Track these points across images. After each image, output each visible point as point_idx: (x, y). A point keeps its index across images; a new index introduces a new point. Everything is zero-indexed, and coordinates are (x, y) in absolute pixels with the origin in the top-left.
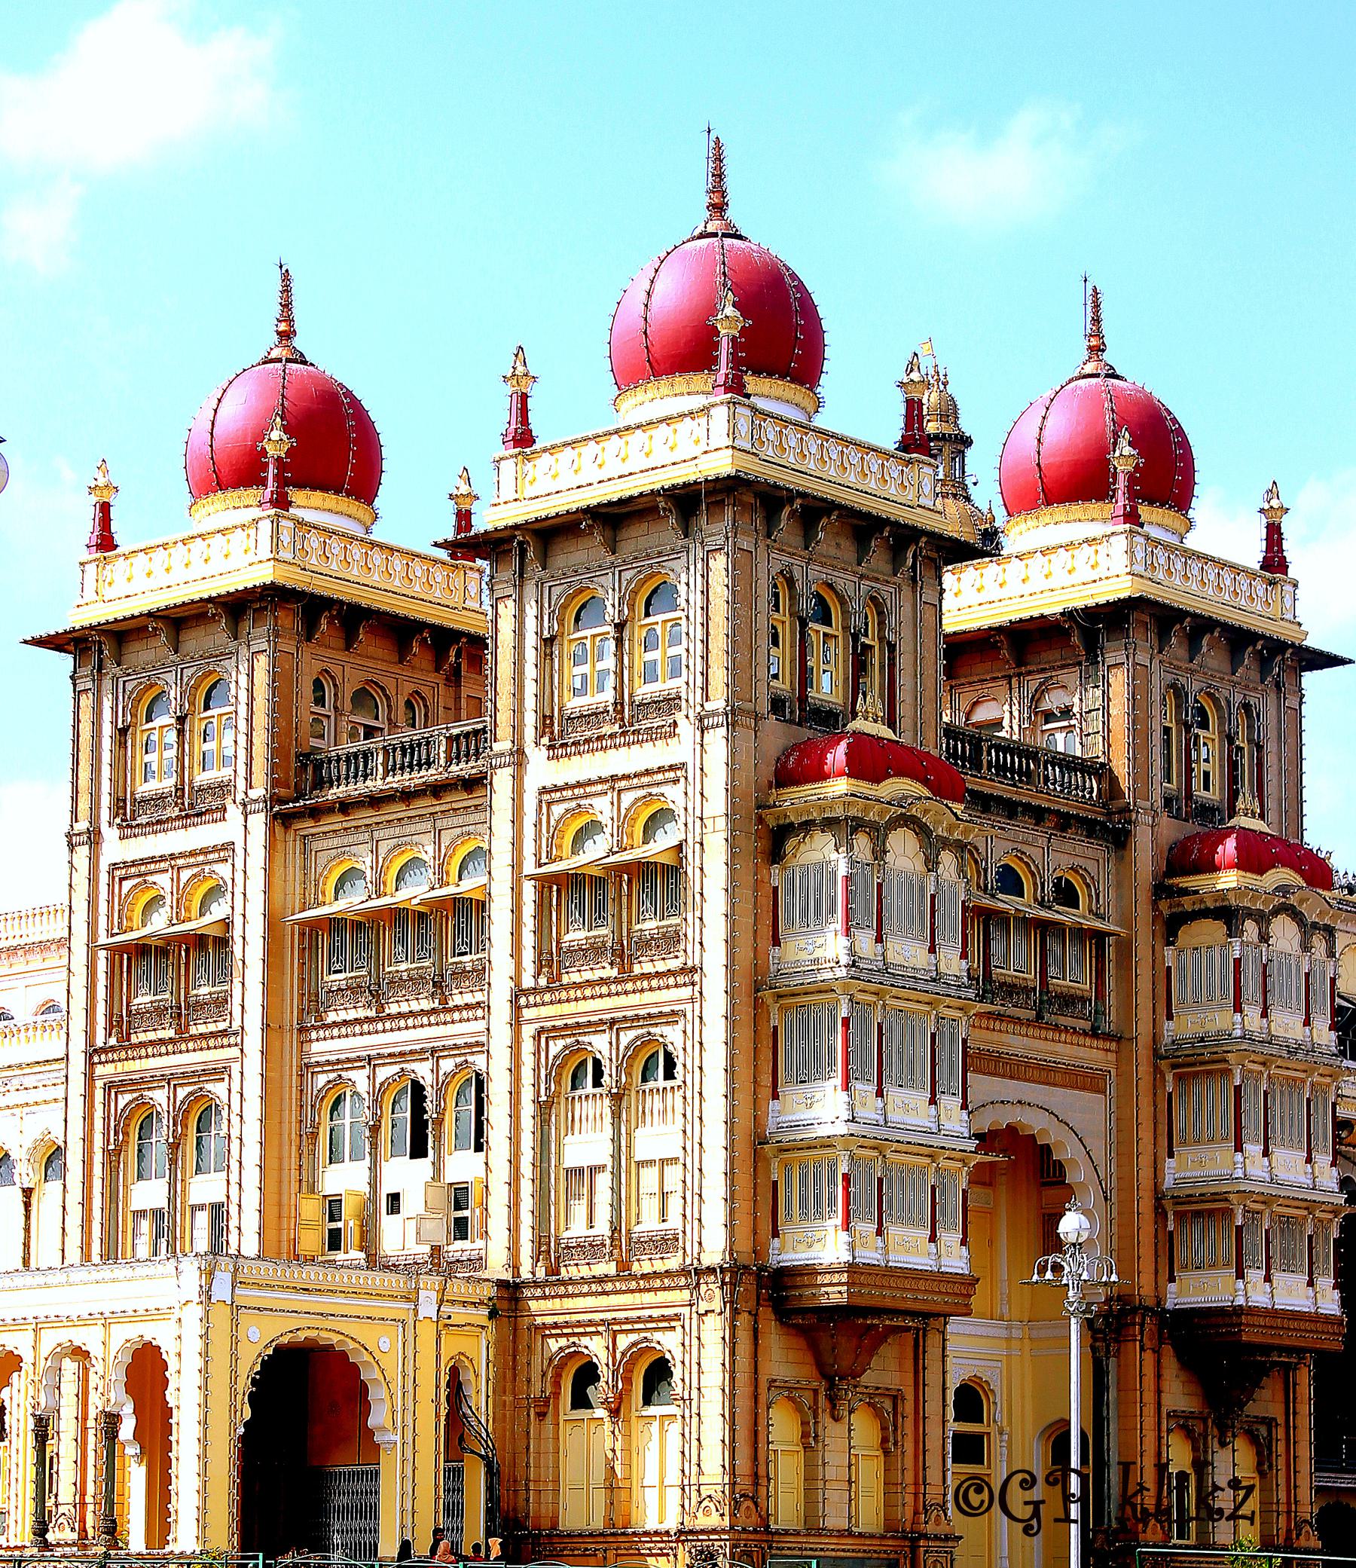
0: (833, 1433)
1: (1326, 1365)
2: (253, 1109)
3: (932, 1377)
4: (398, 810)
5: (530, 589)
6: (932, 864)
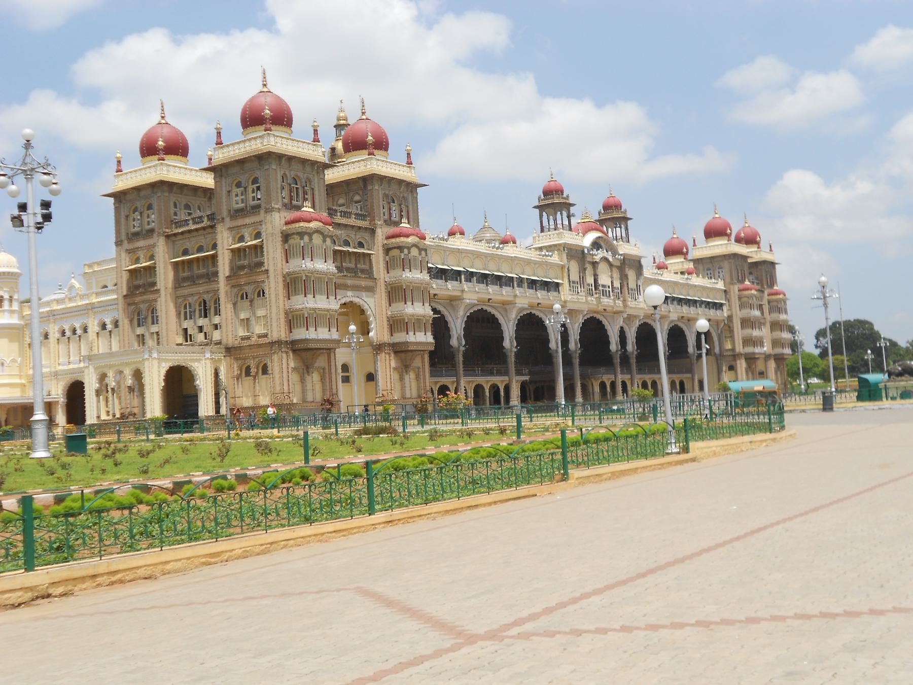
0: (308, 379)
1: (431, 353)
3: (333, 363)
4: (195, 234)
5: (224, 180)
6: (324, 241)
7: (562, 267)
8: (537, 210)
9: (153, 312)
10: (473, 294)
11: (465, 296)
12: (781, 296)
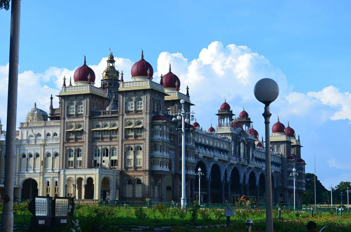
0: (156, 188)
2: (87, 150)
4: (106, 119)
7: (229, 143)
8: (217, 116)
9: (78, 151)
10: (202, 153)
11: (199, 155)
12: (303, 163)
